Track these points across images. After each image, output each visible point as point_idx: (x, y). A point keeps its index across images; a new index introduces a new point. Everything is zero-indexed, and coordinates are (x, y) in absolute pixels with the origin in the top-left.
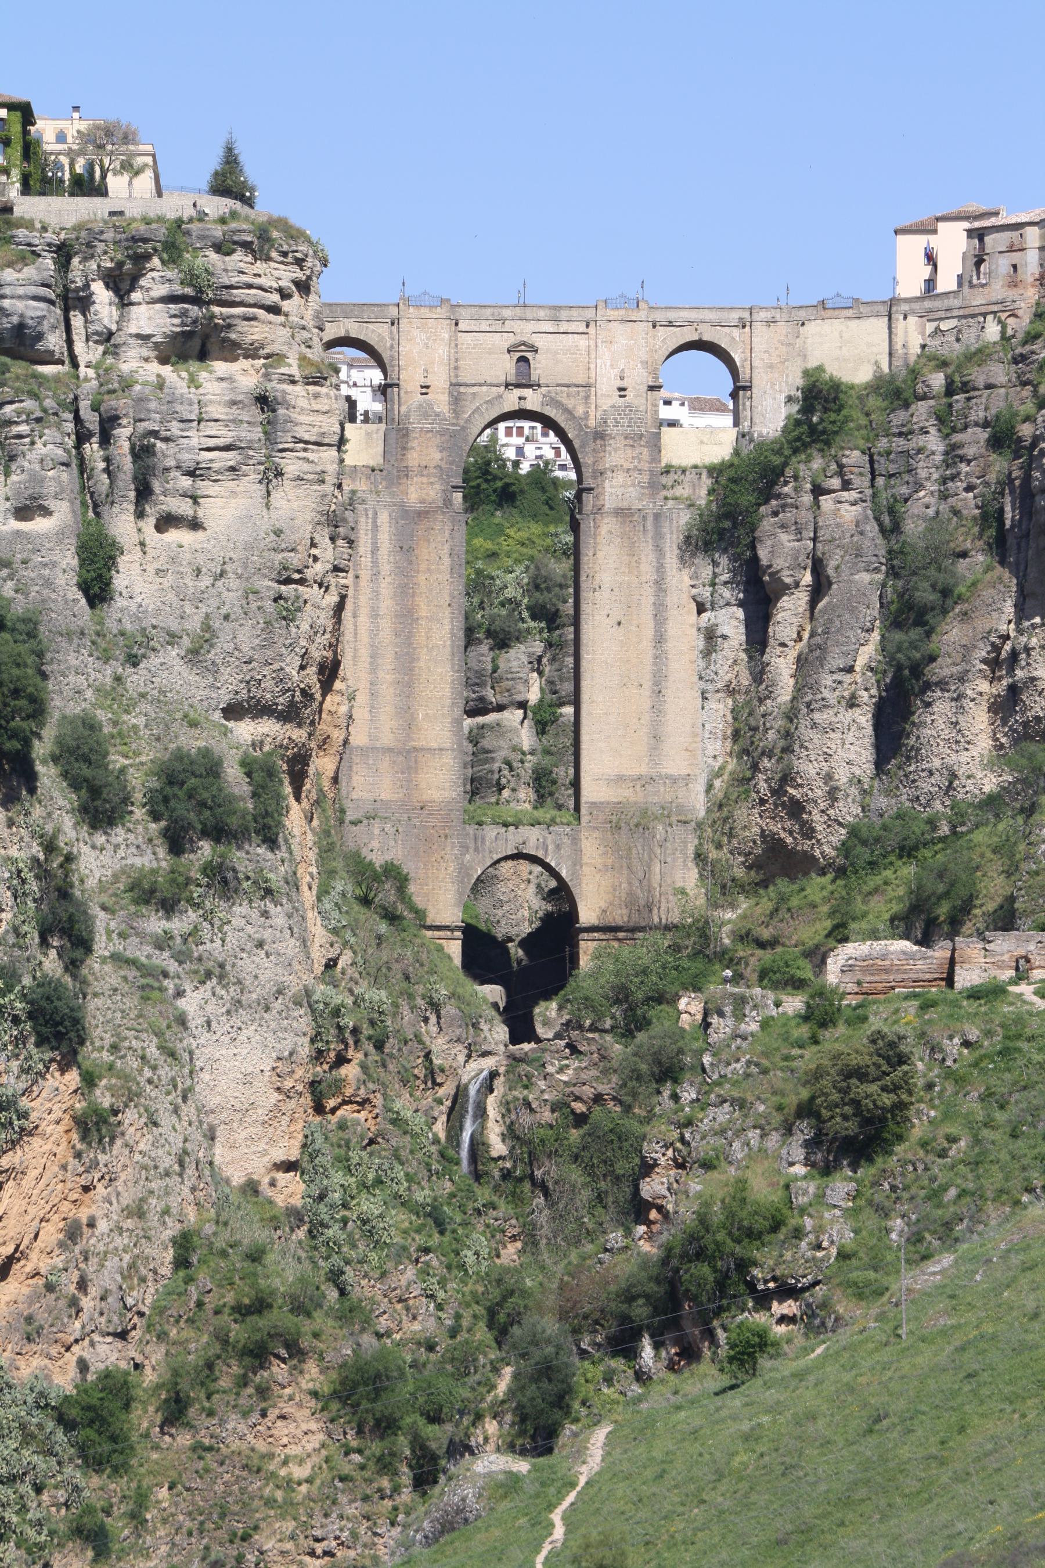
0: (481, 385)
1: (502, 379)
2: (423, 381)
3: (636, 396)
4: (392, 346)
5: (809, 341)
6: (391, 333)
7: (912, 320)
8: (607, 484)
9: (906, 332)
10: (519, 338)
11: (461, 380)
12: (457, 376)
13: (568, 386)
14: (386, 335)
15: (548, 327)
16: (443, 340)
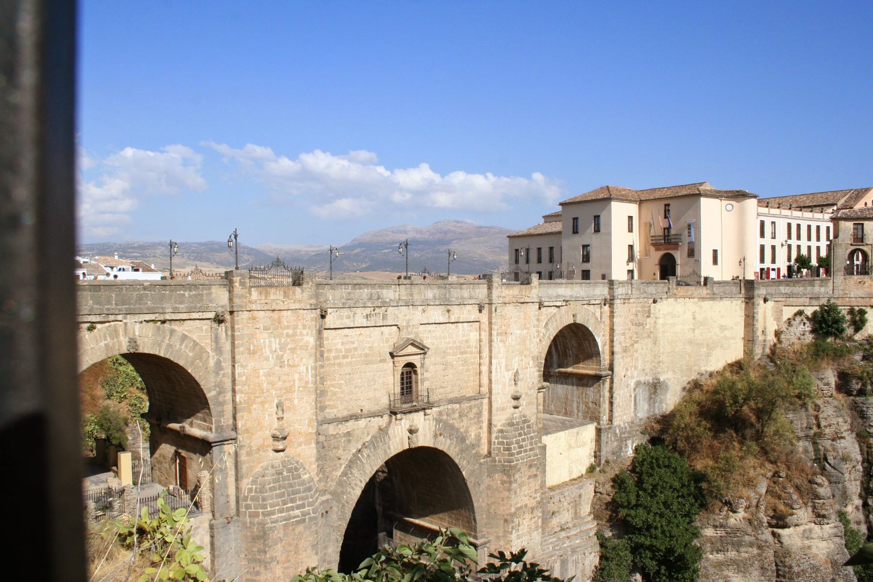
0: (355, 417)
1: (385, 402)
2: (276, 424)
3: (529, 403)
4: (219, 365)
5: (660, 321)
6: (217, 339)
7: (770, 304)
8: (514, 536)
9: (765, 317)
10: (405, 335)
11: (331, 413)
12: (322, 408)
13: (458, 401)
14: (207, 343)
15: (437, 314)
16: (305, 347)
